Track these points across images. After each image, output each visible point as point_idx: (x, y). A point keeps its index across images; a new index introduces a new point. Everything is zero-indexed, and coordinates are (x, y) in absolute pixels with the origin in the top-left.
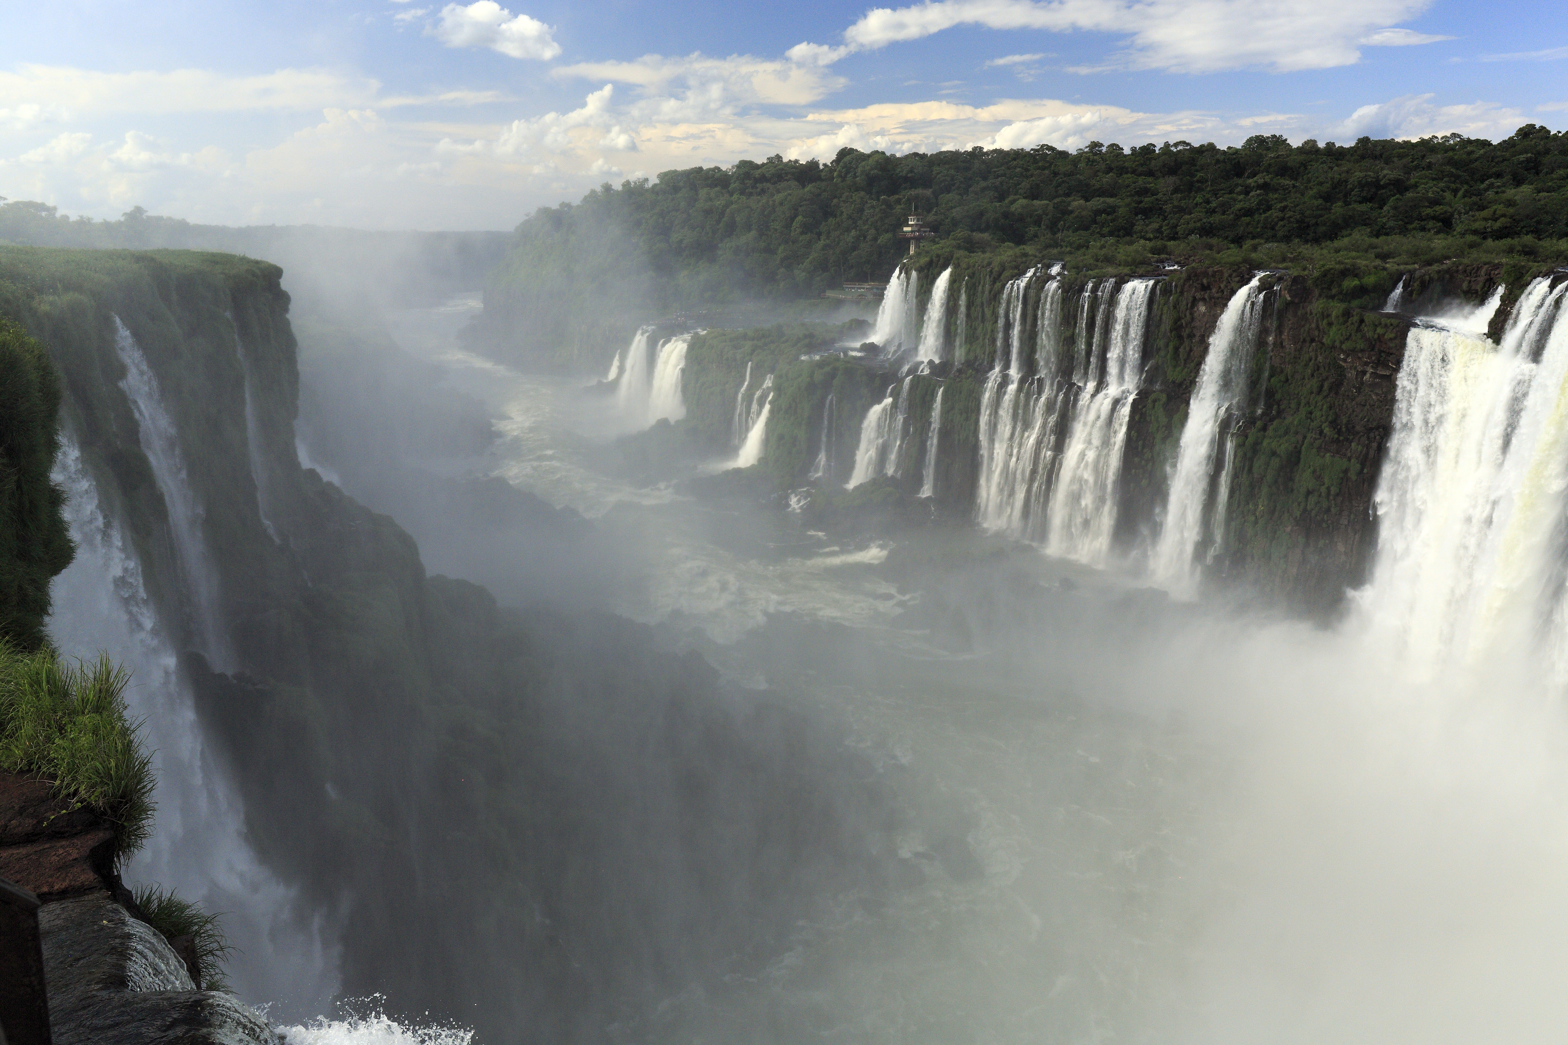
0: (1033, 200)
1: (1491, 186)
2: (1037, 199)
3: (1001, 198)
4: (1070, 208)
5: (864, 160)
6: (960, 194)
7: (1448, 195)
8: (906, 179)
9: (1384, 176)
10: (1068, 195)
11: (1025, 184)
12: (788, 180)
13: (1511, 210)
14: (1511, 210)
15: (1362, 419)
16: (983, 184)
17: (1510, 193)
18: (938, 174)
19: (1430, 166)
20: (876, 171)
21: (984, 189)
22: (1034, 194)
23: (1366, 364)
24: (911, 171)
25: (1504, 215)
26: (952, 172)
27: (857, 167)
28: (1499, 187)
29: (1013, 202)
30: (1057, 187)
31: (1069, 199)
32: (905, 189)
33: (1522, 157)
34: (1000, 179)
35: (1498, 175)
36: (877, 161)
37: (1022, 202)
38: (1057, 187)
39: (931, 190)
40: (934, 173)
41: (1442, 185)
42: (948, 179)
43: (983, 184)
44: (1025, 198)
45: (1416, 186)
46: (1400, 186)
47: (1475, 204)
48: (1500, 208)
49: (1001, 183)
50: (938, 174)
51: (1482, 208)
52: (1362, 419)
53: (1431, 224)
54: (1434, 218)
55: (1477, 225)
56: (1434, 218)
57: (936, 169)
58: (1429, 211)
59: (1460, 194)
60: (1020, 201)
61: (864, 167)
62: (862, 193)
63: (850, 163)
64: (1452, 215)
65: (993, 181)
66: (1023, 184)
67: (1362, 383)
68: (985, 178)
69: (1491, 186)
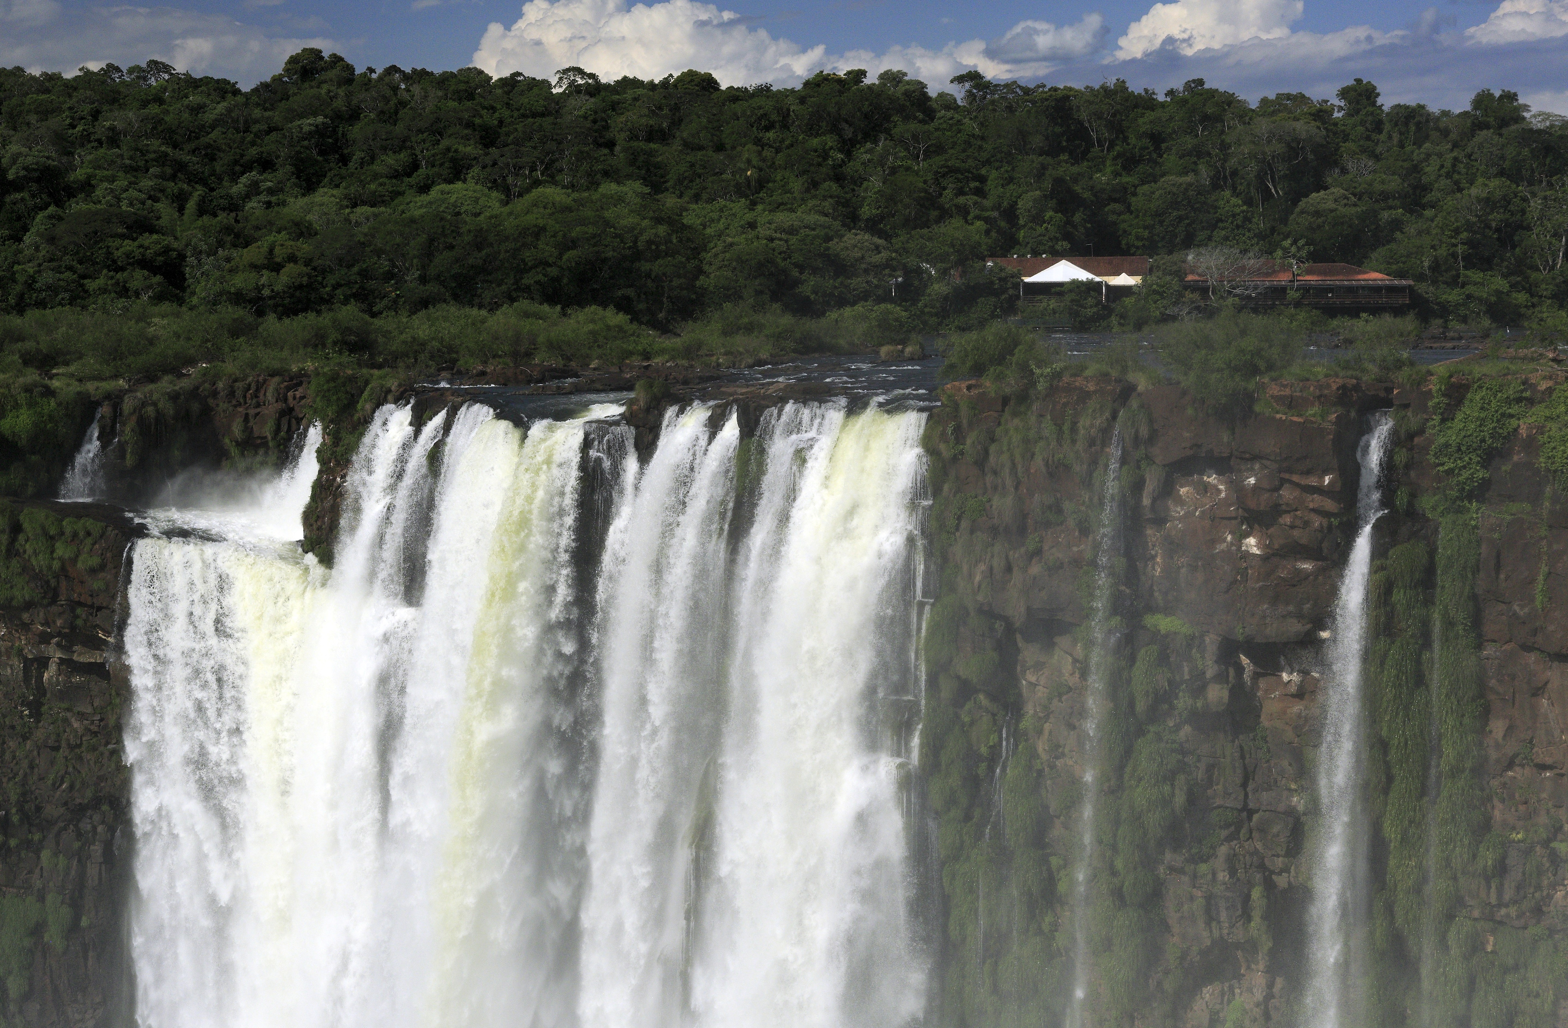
1: (254, 189)
7: (165, 210)
9: (14, 160)
13: (305, 247)
14: (305, 247)
15: (55, 786)
17: (296, 205)
19: (114, 138)
23: (45, 638)
25: (292, 258)
28: (271, 191)
33: (308, 123)
35: (266, 164)
41: (147, 183)
45: (87, 187)
46: (53, 186)
47: (228, 230)
48: (282, 243)
51: (243, 241)
52: (55, 786)
53: (137, 278)
54: (144, 263)
55: (240, 281)
56: (144, 263)
58: (128, 246)
59: (191, 205)
64: (182, 257)
67: (41, 690)
69: (254, 189)
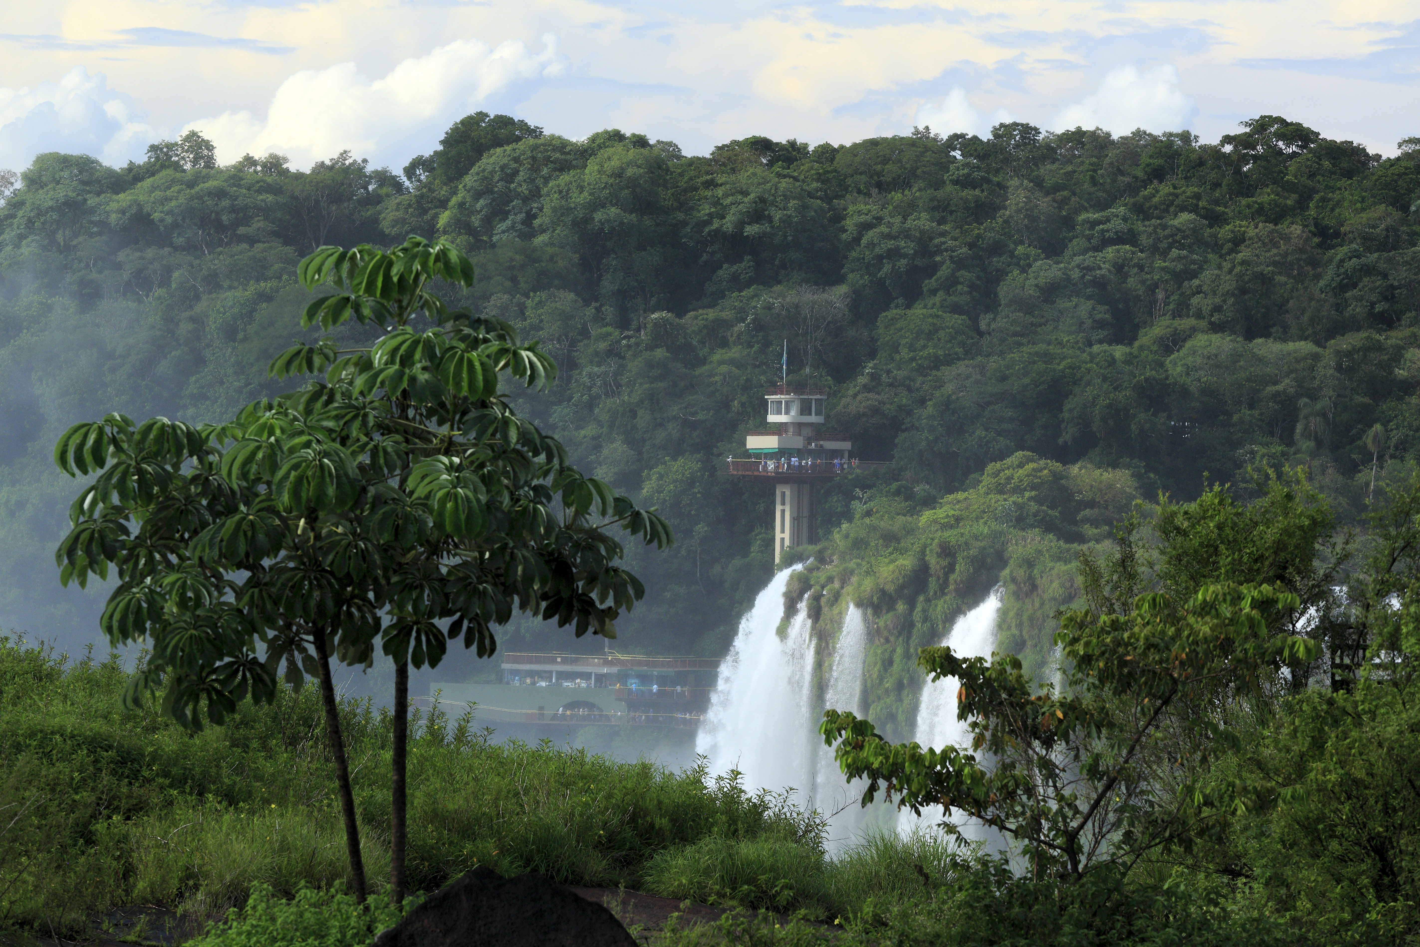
0: (1250, 336)
2: (1266, 334)
3: (1123, 326)
4: (1401, 373)
5: (563, 167)
6: (956, 309)
8: (736, 244)
10: (1387, 321)
11: (1217, 278)
12: (252, 241)
16: (1046, 270)
18: (867, 226)
20: (613, 211)
21: (1051, 292)
22: (1255, 315)
24: (757, 215)
26: (922, 221)
27: (536, 194)
29: (1172, 343)
30: (1343, 288)
31: (1393, 338)
32: (737, 283)
34: (1110, 252)
36: (618, 174)
37: (1208, 344)
38: (1343, 288)
39: (843, 289)
40: (850, 224)
42: (908, 247)
43: (1046, 270)
44: (1216, 328)
49: (1120, 268)
50: (867, 226)
57: (857, 210)
60: (1201, 340)
61: (564, 194)
62: (566, 299)
63: (510, 177)
65: (1088, 259)
66: (1208, 274)
68: (1053, 249)
